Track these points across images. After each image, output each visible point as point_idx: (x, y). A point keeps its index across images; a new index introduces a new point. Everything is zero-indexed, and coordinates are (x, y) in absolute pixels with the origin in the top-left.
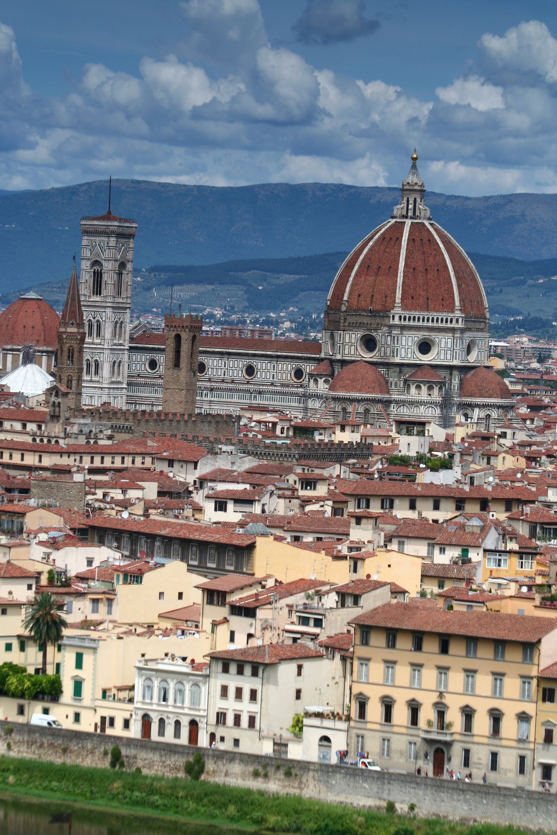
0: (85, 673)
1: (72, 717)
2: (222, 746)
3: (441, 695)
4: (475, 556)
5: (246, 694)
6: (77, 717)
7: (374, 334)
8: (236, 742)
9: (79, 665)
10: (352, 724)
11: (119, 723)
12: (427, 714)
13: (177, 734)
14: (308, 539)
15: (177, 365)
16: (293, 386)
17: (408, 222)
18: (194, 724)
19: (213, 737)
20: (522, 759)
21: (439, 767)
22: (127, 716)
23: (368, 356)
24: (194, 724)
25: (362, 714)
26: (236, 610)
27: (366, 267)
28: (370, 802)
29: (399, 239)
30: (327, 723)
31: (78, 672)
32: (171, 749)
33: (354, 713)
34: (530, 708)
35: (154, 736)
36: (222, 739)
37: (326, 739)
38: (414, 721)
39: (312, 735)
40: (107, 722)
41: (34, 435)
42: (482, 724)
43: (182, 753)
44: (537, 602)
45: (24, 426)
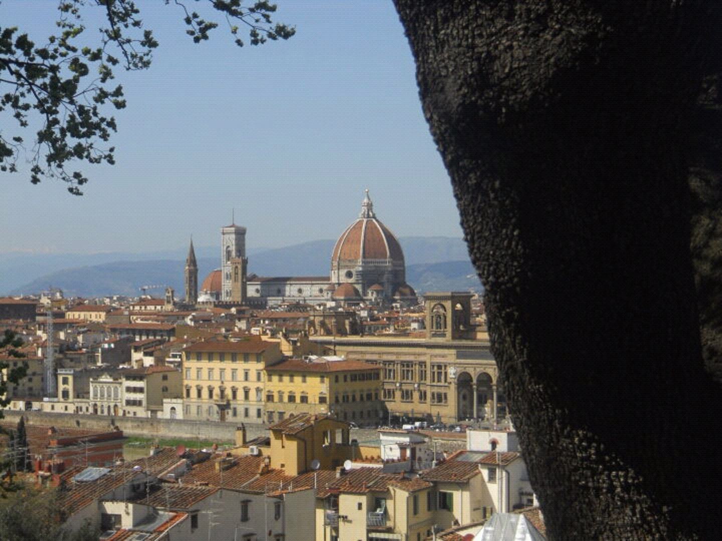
1: (64, 408)
2: (127, 415)
3: (222, 383)
6: (66, 408)
7: (352, 270)
8: (135, 413)
9: (65, 381)
10: (185, 400)
11: (84, 409)
12: (216, 391)
16: (318, 296)
17: (365, 220)
18: (116, 406)
19: (124, 411)
20: (259, 410)
21: (223, 418)
22: (87, 405)
23: (351, 281)
24: (116, 406)
25: (188, 395)
26: (146, 354)
27: (348, 240)
28: (188, 436)
29: (361, 228)
30: (174, 400)
31: (66, 386)
32: (101, 418)
33: (185, 395)
34: (260, 385)
35: (99, 413)
36: (129, 412)
37: (173, 409)
38: (211, 396)
39: (167, 407)
40: (79, 409)
42: (240, 394)
43: (105, 420)
44: (269, 336)
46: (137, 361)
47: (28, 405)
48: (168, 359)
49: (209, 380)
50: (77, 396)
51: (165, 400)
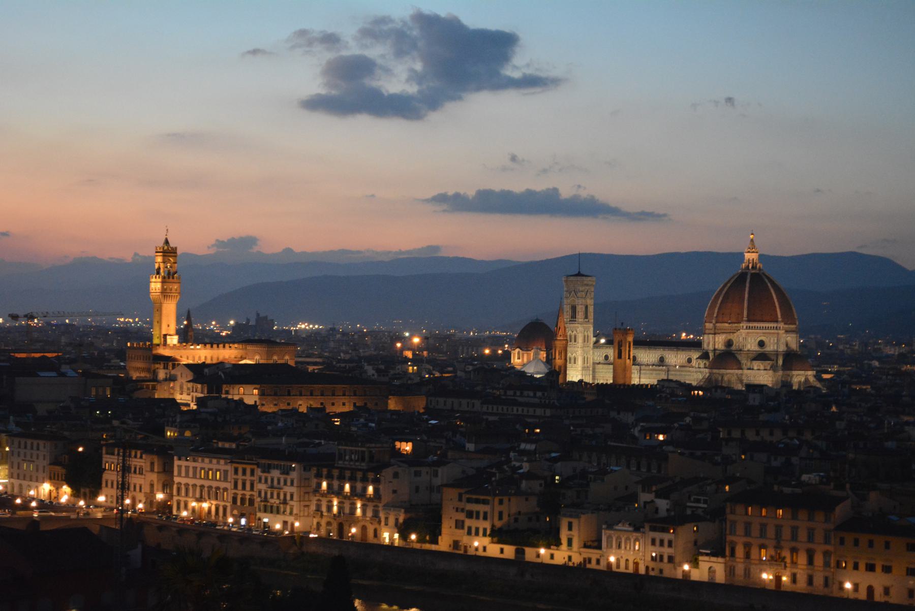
0: (575, 533)
2: (652, 573)
4: (795, 460)
5: (666, 543)
6: (570, 558)
8: (661, 571)
9: (570, 528)
11: (594, 562)
13: (627, 568)
14: (699, 453)
15: (620, 356)
19: (647, 568)
20: (826, 579)
25: (733, 553)
26: (658, 496)
30: (713, 559)
41: (540, 398)
45: (535, 394)
46: (645, 503)
47: (520, 553)
48: (689, 504)
49: (761, 536)
50: (585, 546)
51: (701, 558)
